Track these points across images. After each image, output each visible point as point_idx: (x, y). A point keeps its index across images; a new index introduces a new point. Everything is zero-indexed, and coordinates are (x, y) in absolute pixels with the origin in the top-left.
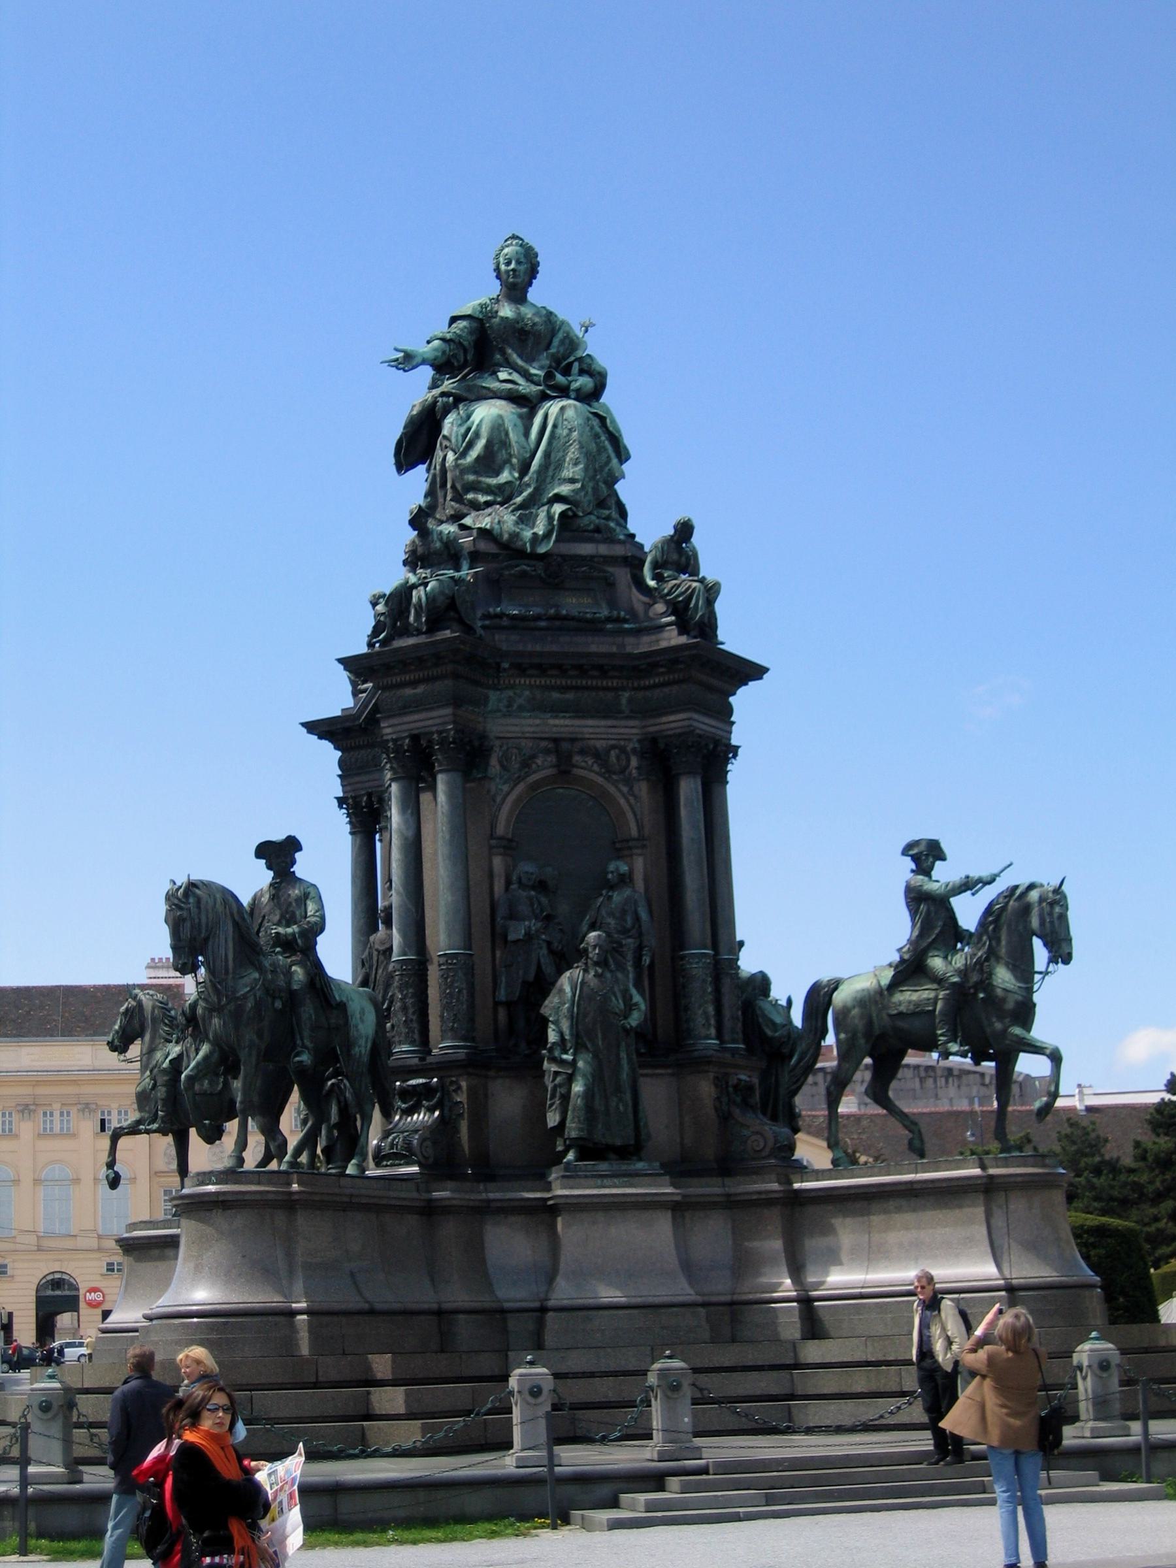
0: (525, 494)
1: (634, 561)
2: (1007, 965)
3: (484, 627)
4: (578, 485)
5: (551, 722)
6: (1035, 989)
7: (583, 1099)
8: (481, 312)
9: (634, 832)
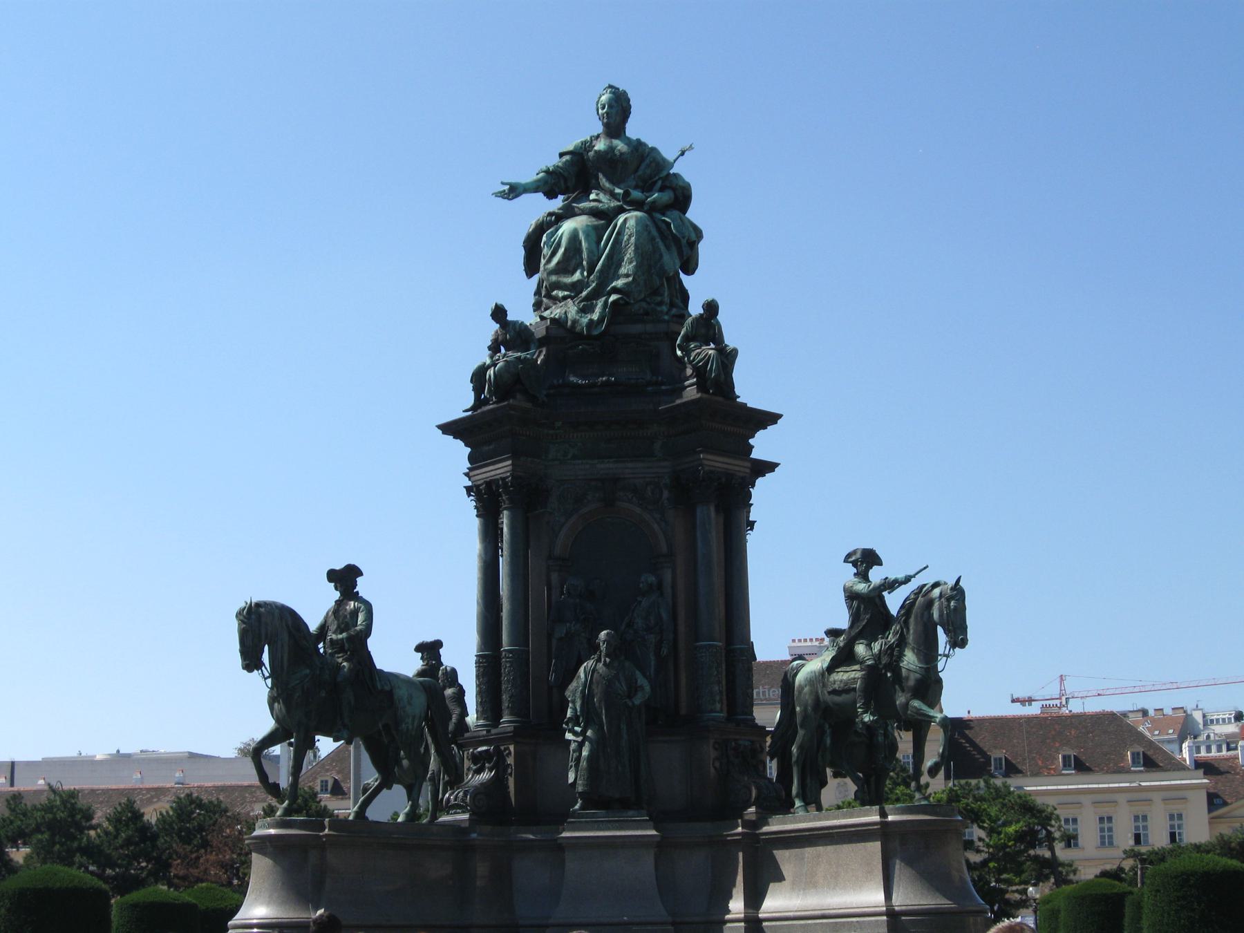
0: (589, 289)
2: (913, 650)
3: (547, 396)
4: (631, 279)
6: (939, 670)
7: (587, 762)
8: (581, 148)
9: (664, 548)
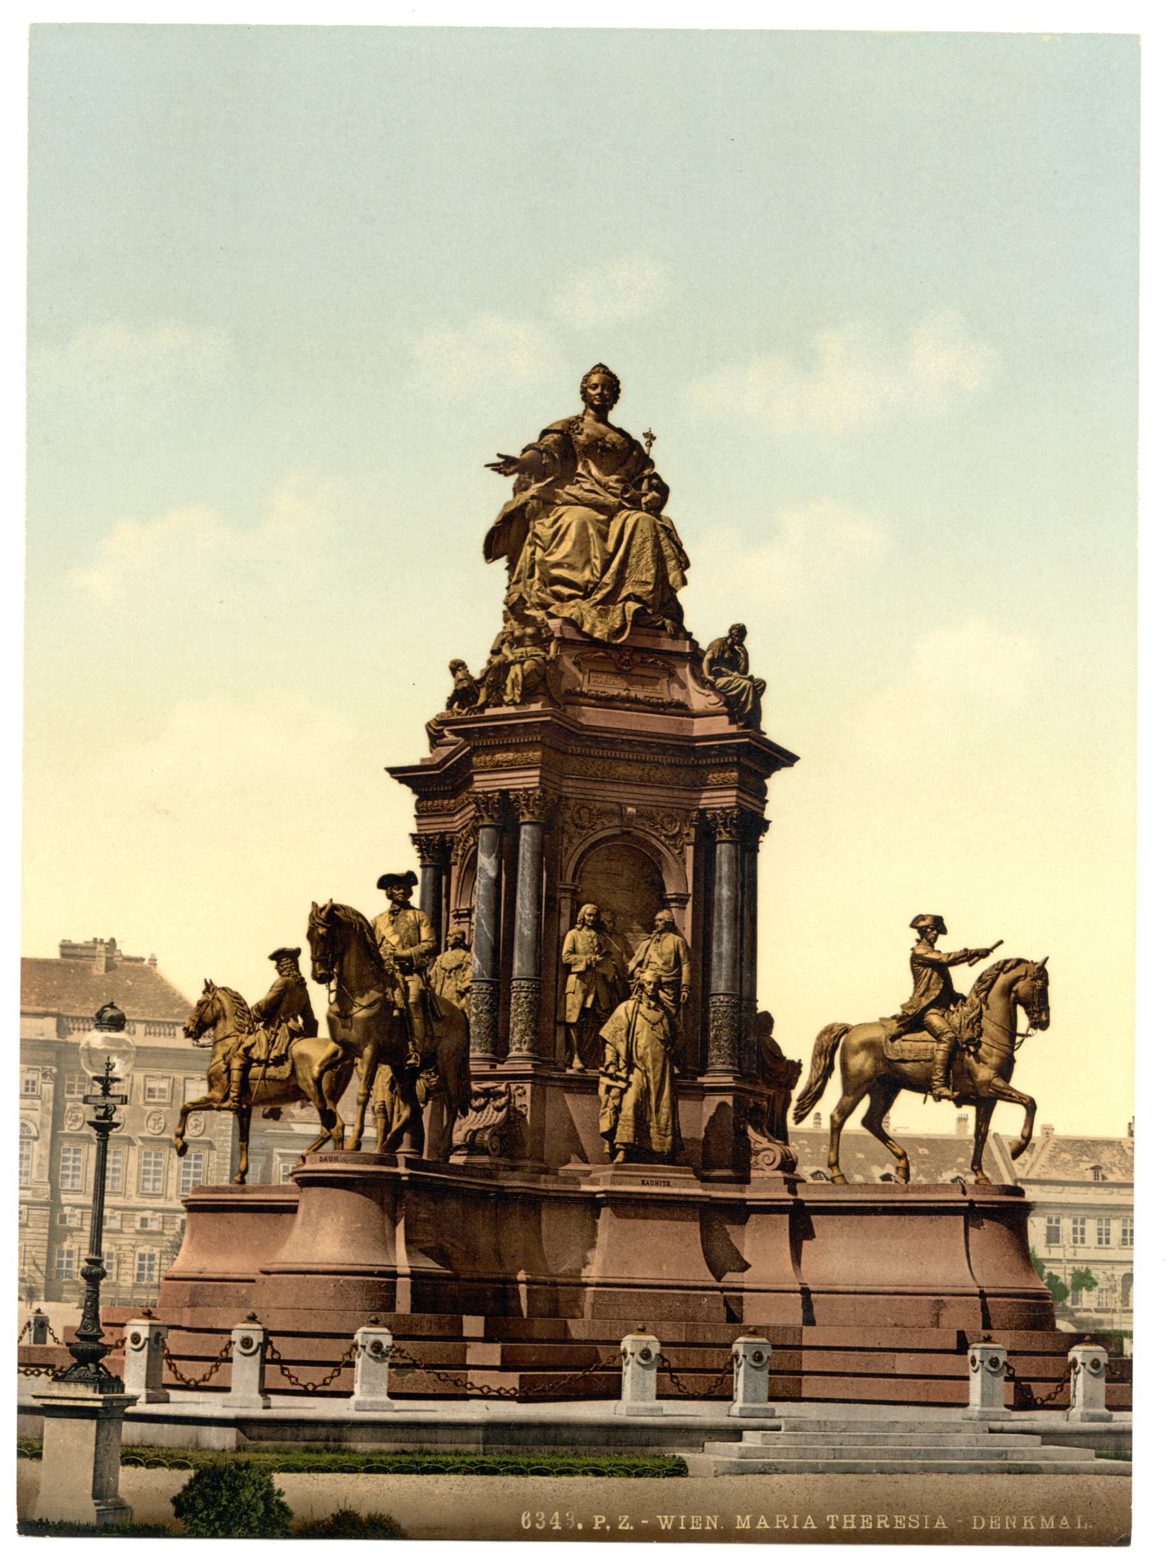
1: (696, 655)
4: (650, 588)
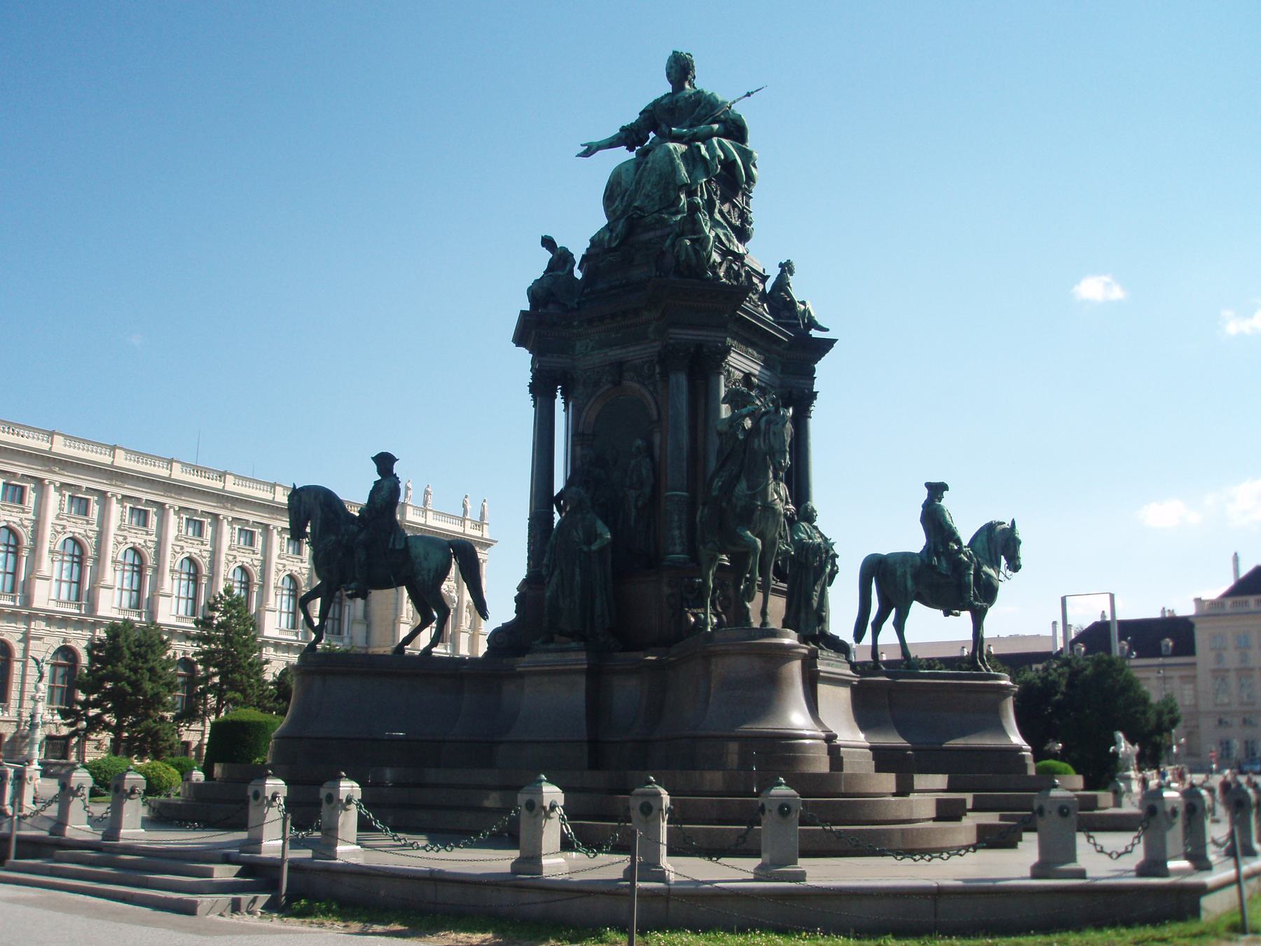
5: (610, 354)
